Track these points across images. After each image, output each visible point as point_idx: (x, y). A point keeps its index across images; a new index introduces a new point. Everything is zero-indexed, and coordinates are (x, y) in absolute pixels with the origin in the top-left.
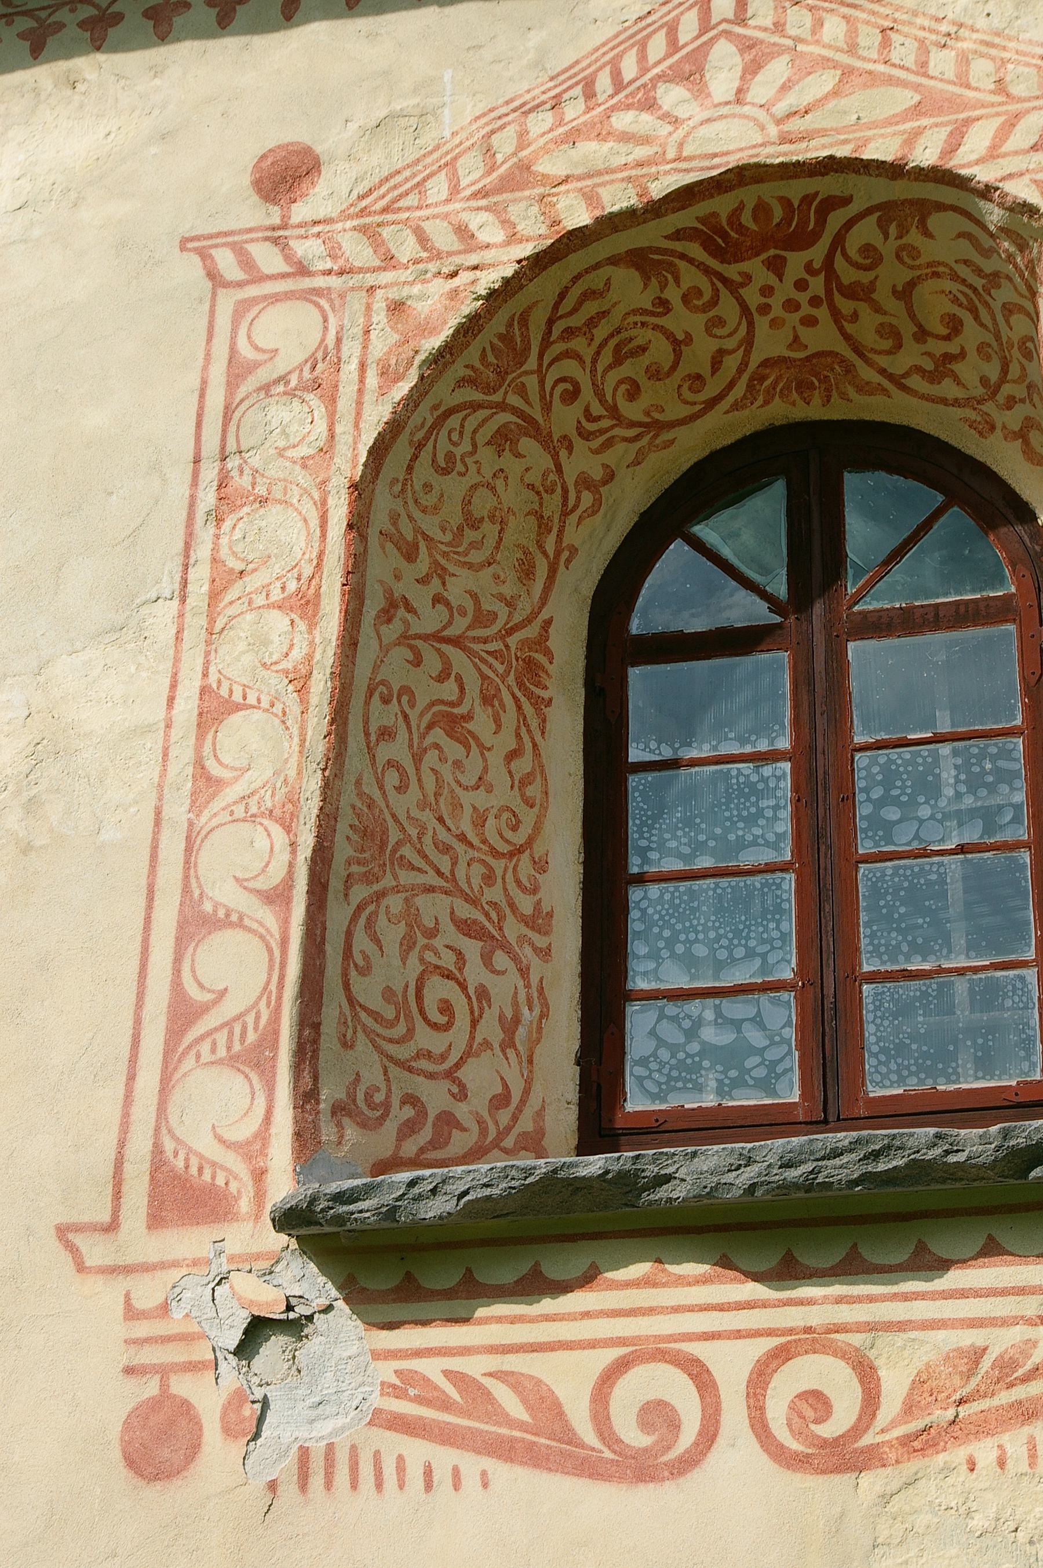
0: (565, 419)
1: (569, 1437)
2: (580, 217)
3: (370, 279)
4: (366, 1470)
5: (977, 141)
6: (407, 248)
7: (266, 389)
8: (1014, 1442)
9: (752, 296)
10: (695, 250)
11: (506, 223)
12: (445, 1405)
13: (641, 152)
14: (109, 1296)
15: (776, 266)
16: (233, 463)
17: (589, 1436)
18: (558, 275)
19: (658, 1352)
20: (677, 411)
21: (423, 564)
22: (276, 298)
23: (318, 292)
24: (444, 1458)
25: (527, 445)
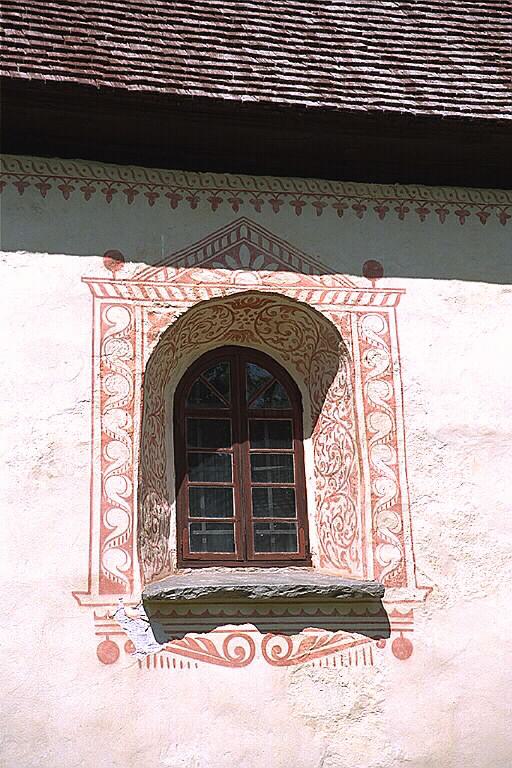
2: (206, 297)
3: (141, 303)
4: (165, 663)
5: (316, 297)
6: (153, 296)
7: (113, 335)
8: (323, 659)
9: (237, 316)
10: (230, 307)
13: (223, 279)
16: (104, 358)
17: (223, 655)
23: (126, 304)
24: (185, 660)
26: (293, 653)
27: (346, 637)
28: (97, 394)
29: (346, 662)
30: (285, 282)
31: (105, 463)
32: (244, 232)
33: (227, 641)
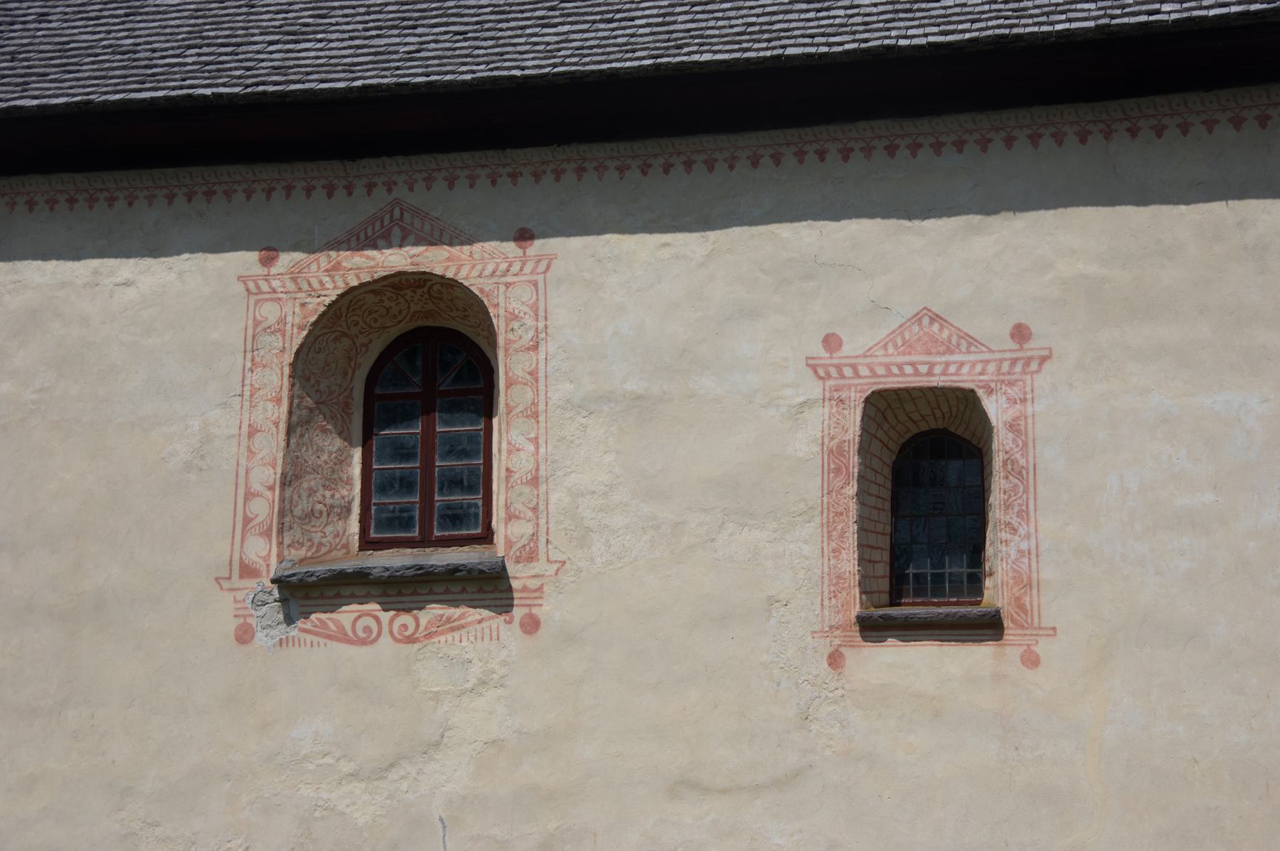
0: (354, 331)
1: (346, 634)
2: (355, 283)
5: (463, 273)
6: (305, 287)
7: (265, 330)
8: (449, 637)
11: (334, 282)
12: (316, 626)
13: (372, 263)
14: (229, 596)
15: (415, 292)
17: (350, 634)
18: (349, 297)
19: (368, 614)
20: (389, 324)
21: (313, 381)
22: (266, 300)
23: (280, 299)
24: (316, 639)
25: (344, 340)
26: (422, 628)
27: (474, 614)
28: (247, 388)
29: (472, 638)
30: (435, 259)
31: (251, 453)
32: (397, 212)
33: (356, 620)
